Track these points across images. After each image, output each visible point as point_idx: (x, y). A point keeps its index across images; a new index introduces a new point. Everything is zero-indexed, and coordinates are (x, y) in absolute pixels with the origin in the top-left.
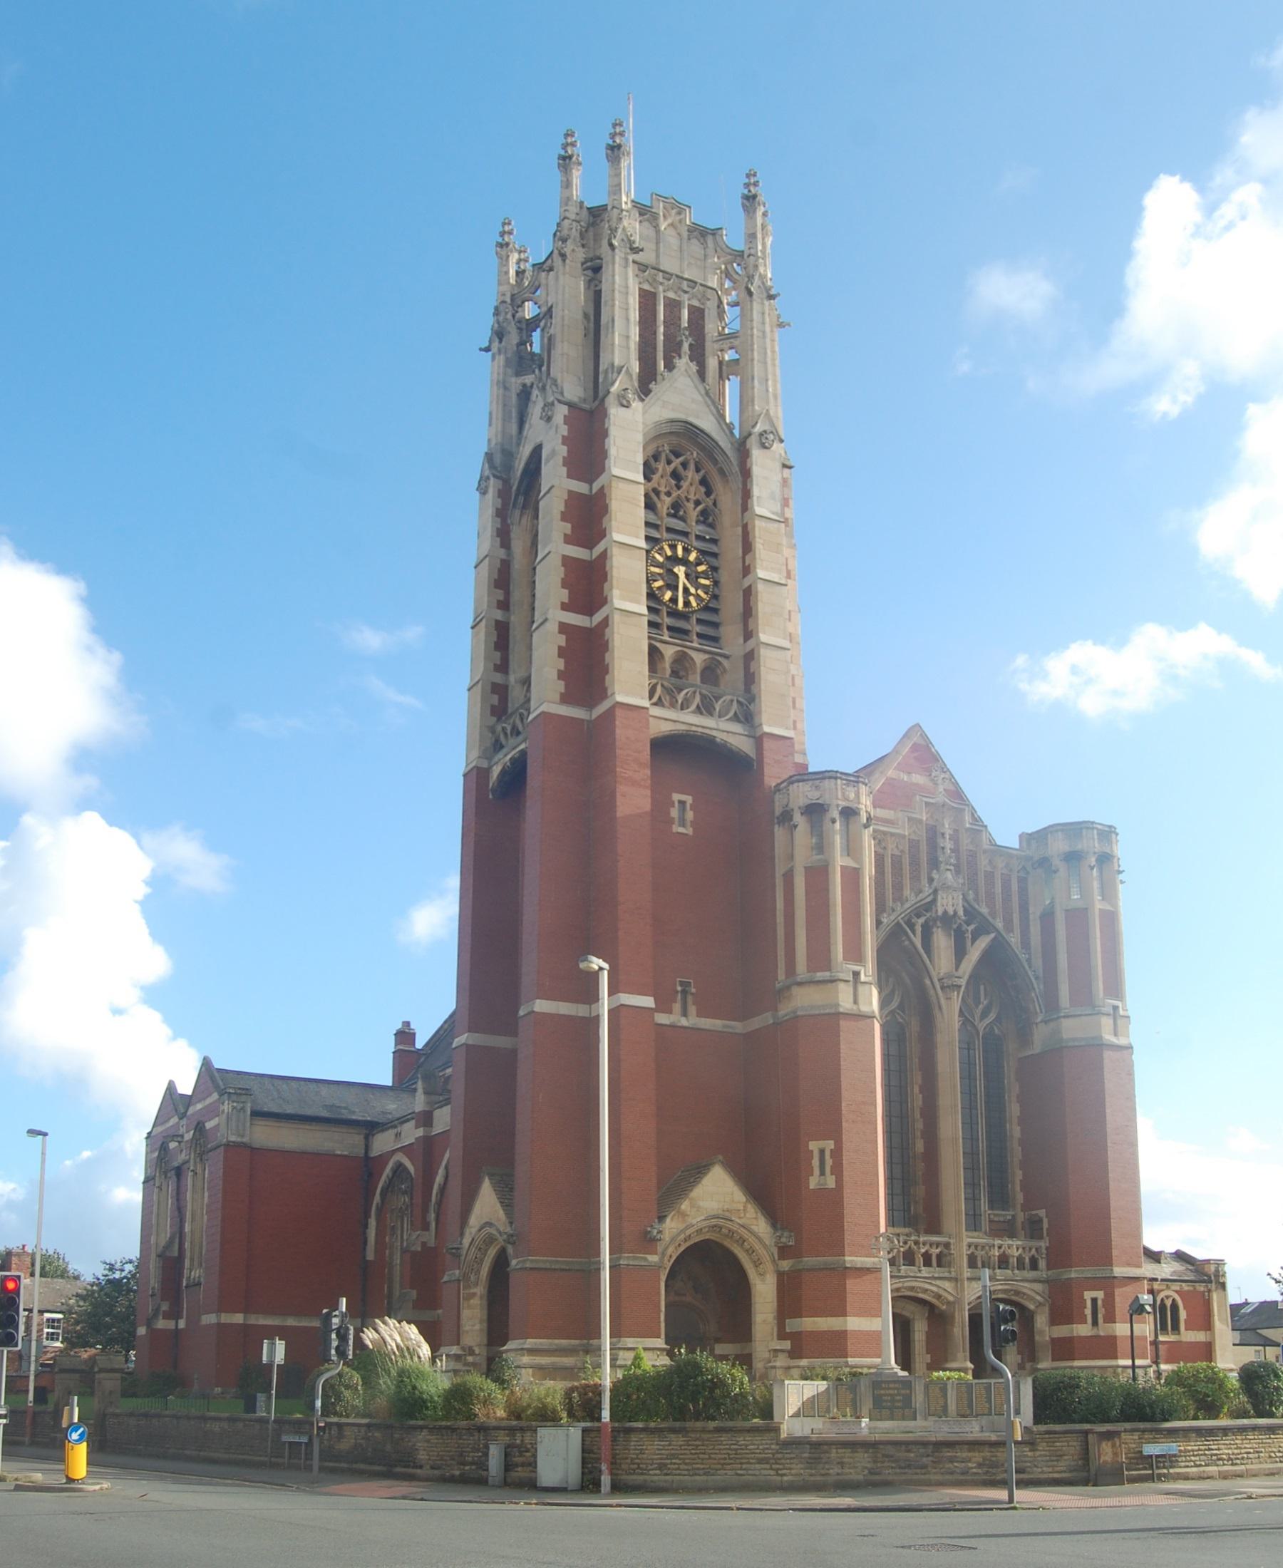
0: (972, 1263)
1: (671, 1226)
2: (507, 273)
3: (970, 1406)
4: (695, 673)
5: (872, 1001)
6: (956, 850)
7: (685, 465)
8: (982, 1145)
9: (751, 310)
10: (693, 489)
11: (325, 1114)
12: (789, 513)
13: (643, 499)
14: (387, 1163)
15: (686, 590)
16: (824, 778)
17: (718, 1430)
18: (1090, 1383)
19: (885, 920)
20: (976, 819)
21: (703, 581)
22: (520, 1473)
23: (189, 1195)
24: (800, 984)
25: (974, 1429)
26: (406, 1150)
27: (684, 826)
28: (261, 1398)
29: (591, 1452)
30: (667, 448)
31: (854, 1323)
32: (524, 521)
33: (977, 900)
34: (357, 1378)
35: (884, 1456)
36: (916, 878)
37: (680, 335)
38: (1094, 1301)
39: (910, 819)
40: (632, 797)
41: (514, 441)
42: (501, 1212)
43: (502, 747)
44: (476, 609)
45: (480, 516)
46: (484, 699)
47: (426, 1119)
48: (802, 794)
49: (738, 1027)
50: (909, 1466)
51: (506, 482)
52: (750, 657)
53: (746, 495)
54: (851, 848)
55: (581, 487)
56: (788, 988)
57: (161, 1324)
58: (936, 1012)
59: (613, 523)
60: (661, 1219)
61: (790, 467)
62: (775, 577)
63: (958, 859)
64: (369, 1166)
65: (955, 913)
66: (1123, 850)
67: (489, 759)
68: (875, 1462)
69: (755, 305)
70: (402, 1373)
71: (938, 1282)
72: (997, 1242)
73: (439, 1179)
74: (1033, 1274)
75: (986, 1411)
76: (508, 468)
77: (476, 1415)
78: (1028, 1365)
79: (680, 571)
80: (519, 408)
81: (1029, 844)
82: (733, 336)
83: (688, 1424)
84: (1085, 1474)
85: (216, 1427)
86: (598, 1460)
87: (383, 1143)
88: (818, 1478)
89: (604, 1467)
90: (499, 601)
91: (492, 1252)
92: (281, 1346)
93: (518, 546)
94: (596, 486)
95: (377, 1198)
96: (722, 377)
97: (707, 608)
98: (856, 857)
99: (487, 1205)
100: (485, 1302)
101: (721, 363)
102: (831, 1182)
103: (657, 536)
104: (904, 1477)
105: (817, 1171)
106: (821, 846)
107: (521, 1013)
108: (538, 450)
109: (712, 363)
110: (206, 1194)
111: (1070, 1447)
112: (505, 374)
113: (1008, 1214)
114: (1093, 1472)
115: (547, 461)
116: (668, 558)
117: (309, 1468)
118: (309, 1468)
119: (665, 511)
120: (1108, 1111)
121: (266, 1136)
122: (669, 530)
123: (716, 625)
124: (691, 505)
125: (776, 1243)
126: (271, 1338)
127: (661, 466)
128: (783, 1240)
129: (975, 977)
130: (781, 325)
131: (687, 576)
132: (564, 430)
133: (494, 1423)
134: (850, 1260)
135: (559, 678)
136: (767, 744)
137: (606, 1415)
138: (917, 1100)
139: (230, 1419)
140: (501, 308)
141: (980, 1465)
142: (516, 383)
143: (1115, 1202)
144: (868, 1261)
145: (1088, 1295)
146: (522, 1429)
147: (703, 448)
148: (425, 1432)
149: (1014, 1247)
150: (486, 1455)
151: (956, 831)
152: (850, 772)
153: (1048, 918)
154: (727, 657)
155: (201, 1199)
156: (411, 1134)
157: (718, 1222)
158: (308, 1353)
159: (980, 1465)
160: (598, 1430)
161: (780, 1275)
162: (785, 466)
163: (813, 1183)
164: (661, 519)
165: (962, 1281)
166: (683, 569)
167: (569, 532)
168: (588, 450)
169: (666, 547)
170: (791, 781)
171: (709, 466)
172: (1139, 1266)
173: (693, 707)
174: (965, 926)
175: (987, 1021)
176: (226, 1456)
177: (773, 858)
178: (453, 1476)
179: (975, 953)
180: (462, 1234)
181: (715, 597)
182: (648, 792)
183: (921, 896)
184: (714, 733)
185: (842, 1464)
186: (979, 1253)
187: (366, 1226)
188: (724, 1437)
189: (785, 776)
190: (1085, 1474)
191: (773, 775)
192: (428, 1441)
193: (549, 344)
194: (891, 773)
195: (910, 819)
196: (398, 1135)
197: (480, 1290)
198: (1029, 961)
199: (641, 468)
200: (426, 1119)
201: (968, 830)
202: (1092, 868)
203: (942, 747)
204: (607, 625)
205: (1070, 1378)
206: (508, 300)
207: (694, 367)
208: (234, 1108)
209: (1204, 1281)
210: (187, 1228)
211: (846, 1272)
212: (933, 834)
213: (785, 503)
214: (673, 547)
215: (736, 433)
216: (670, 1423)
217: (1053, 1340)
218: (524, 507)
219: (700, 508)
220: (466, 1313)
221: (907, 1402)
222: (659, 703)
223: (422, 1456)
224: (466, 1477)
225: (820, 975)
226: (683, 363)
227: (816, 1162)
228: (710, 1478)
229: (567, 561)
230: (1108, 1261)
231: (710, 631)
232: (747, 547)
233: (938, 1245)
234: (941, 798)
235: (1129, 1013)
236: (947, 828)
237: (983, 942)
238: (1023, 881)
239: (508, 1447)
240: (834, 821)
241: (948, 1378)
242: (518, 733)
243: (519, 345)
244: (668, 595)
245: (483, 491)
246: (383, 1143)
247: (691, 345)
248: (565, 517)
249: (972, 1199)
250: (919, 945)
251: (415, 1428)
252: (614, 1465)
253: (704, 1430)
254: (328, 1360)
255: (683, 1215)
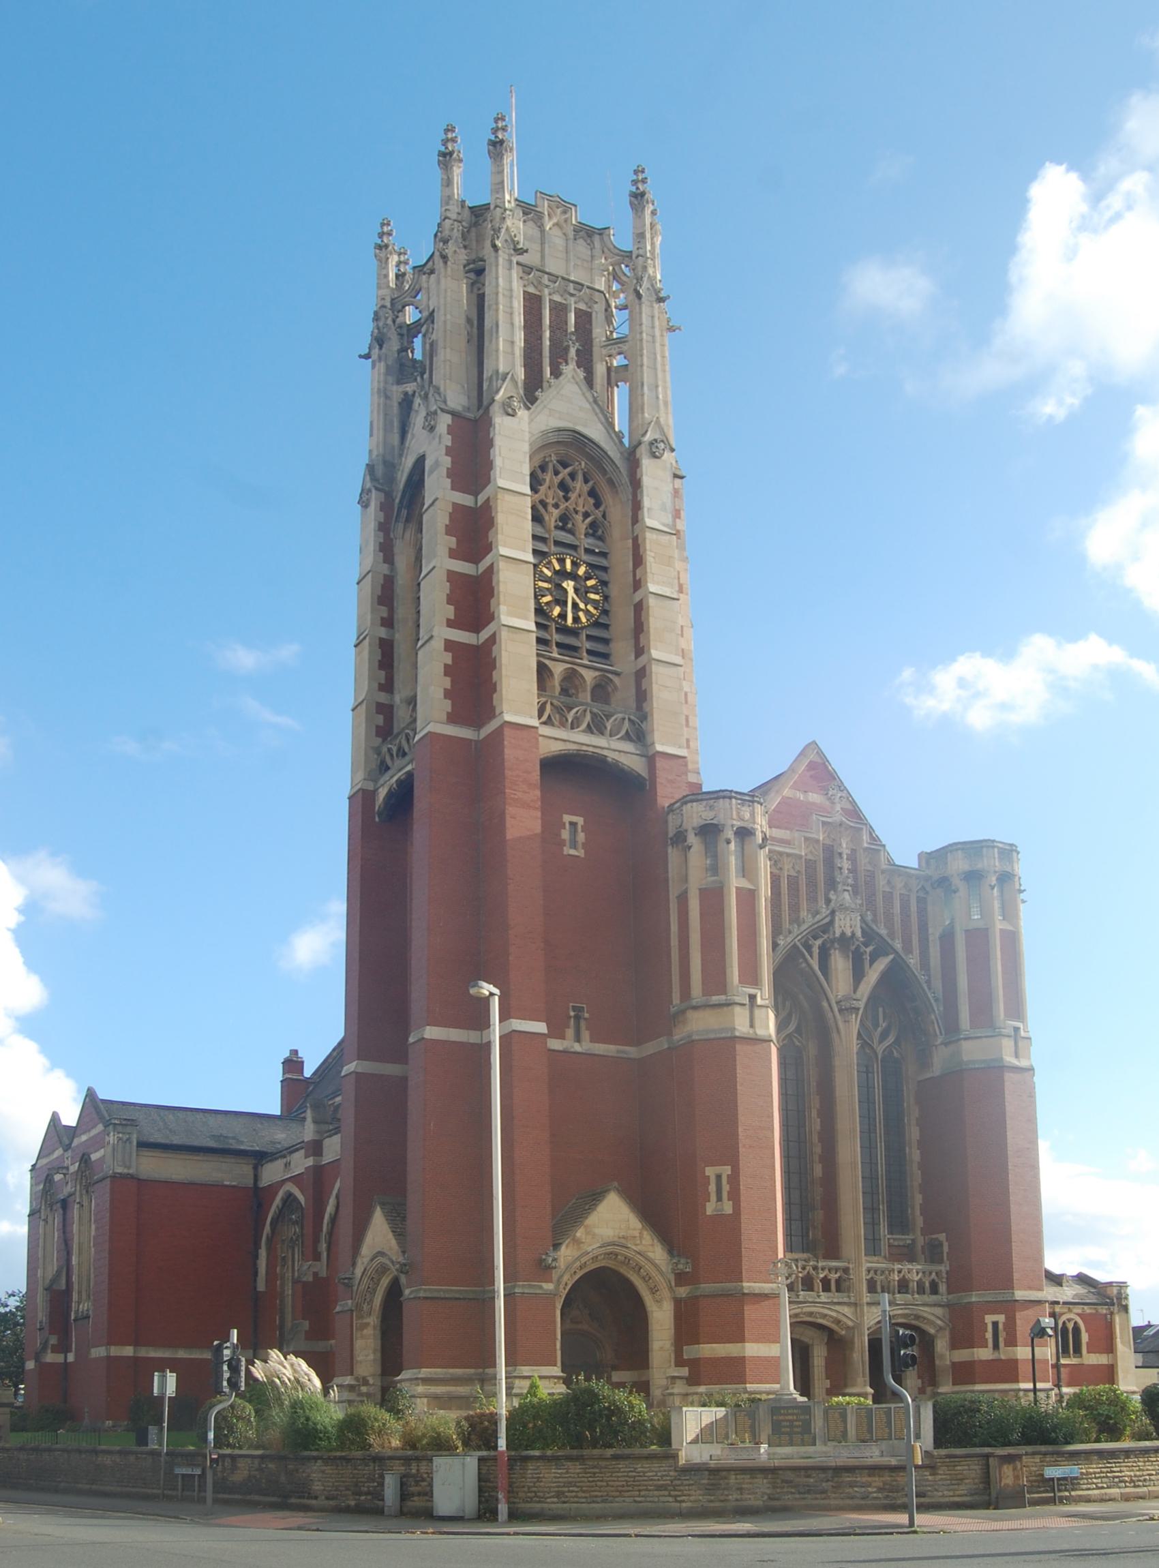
0: (872, 1287)
1: (566, 1254)
2: (386, 276)
3: (870, 1431)
4: (585, 691)
5: (769, 1024)
6: (854, 870)
7: (573, 476)
8: (881, 1168)
9: (641, 313)
10: (581, 501)
11: (212, 1144)
12: (680, 525)
13: (530, 511)
14: (276, 1193)
15: (575, 605)
16: (718, 798)
17: (616, 1457)
18: (990, 1404)
19: (781, 943)
20: (874, 839)
21: (592, 596)
22: (417, 1503)
23: (75, 1227)
24: (695, 1008)
25: (873, 1454)
26: (296, 1180)
27: (575, 848)
28: (153, 1430)
29: (488, 1481)
30: (554, 458)
31: (752, 1349)
32: (407, 535)
33: (875, 921)
34: (249, 1409)
35: (783, 1481)
36: (812, 899)
37: (566, 341)
38: (995, 1324)
39: (806, 839)
40: (522, 818)
41: (396, 451)
42: (394, 1242)
43: (388, 768)
44: (359, 627)
45: (363, 529)
46: (369, 720)
47: (316, 1148)
48: (696, 814)
49: (632, 1052)
50: (809, 1492)
51: (389, 495)
52: (641, 674)
53: (637, 506)
54: (746, 870)
55: (466, 500)
56: (683, 1012)
57: (50, 1358)
58: (835, 1035)
59: (500, 536)
60: (556, 1246)
61: (682, 478)
62: (667, 592)
63: (855, 879)
64: (258, 1196)
65: (853, 934)
66: (1024, 868)
67: (375, 781)
68: (774, 1487)
69: (645, 309)
70: (296, 1405)
71: (837, 1308)
72: (897, 1266)
73: (330, 1209)
74: (934, 1298)
75: (886, 1436)
76: (390, 479)
77: (370, 1446)
78: (929, 1389)
79: (569, 585)
80: (400, 417)
81: (928, 863)
82: (622, 340)
83: (586, 1452)
84: (987, 1498)
85: (107, 1460)
86: (495, 1489)
87: (272, 1173)
88: (717, 1504)
89: (500, 1496)
90: (382, 619)
91: (385, 1282)
92: (171, 1379)
93: (402, 561)
94: (481, 498)
95: (267, 1229)
96: (610, 383)
97: (597, 624)
98: (751, 878)
99: (380, 1233)
100: (378, 1332)
101: (609, 369)
102: (728, 1208)
103: (546, 550)
104: (803, 1503)
105: (713, 1197)
106: (716, 867)
107: (411, 1040)
108: (421, 460)
109: (600, 369)
110: (93, 1227)
111: (971, 1471)
112: (386, 382)
113: (908, 1239)
114: (994, 1494)
115: (431, 472)
116: (556, 572)
117: (202, 1500)
118: (202, 1500)
119: (553, 524)
120: (1009, 1134)
121: (153, 1167)
122: (557, 543)
123: (606, 641)
124: (579, 518)
125: (673, 1270)
126: (162, 1370)
127: (548, 477)
128: (680, 1266)
129: (873, 999)
130: (671, 329)
131: (576, 590)
132: (448, 441)
133: (390, 1453)
134: (748, 1286)
135: (445, 697)
136: (660, 763)
137: (502, 1443)
138: (816, 1124)
139: (120, 1452)
140: (381, 314)
141: (880, 1490)
142: (397, 392)
143: (1017, 1225)
144: (766, 1287)
145: (989, 1319)
146: (417, 1459)
147: (590, 458)
148: (319, 1462)
149: (914, 1271)
150: (382, 1484)
151: (854, 851)
152: (746, 791)
153: (948, 939)
154: (617, 674)
155: (88, 1230)
156: (301, 1163)
157: (614, 1249)
158: (200, 1384)
159: (880, 1490)
160: (495, 1459)
161: (678, 1302)
162: (676, 476)
163: (710, 1208)
164: (549, 531)
165: (862, 1305)
166: (571, 583)
167: (454, 546)
168: (473, 465)
169: (554, 561)
170: (684, 801)
171: (598, 477)
172: (1041, 1289)
173: (584, 726)
174: (863, 948)
175: (886, 1044)
176: (119, 1489)
177: (666, 880)
178: (349, 1506)
179: (873, 975)
180: (354, 1264)
181: (605, 612)
182: (539, 814)
183: (818, 917)
184: (605, 753)
185: (740, 1489)
186: (879, 1278)
187: (256, 1257)
188: (621, 1465)
189: (678, 796)
190: (987, 1498)
191: (666, 795)
192: (323, 1472)
193: (431, 351)
194: (787, 792)
195: (806, 839)
196: (287, 1165)
197: (373, 1320)
198: (928, 982)
199: (528, 478)
200: (316, 1148)
202: (993, 888)
203: (837, 763)
204: (494, 643)
205: (972, 1402)
206: (388, 305)
207: (581, 374)
208: (120, 1139)
209: (1106, 1304)
210: (74, 1261)
211: (744, 1297)
212: (830, 854)
213: (677, 514)
214: (562, 561)
215: (626, 441)
216: (568, 1451)
217: (954, 1364)
218: (407, 521)
219: (589, 520)
220: (359, 1344)
221: (807, 1428)
222: (548, 722)
223: (317, 1487)
224: (361, 1507)
225: (715, 999)
226: (570, 369)
227: (712, 1188)
228: (607, 1505)
229: (452, 576)
230: (1009, 1284)
231: (600, 648)
232: (638, 560)
233: (837, 1270)
234: (838, 817)
235: (1031, 1034)
236: (845, 846)
237: (882, 964)
238: (922, 901)
239: (403, 1476)
240: (728, 842)
241: (848, 1403)
242: (404, 754)
243: (399, 351)
244: (557, 611)
245: (364, 504)
246: (272, 1173)
247: (578, 350)
248: (449, 531)
249: (872, 1224)
250: (816, 967)
251: (309, 1459)
252: (511, 1492)
253: (601, 1458)
254: (220, 1392)
255: (578, 1242)
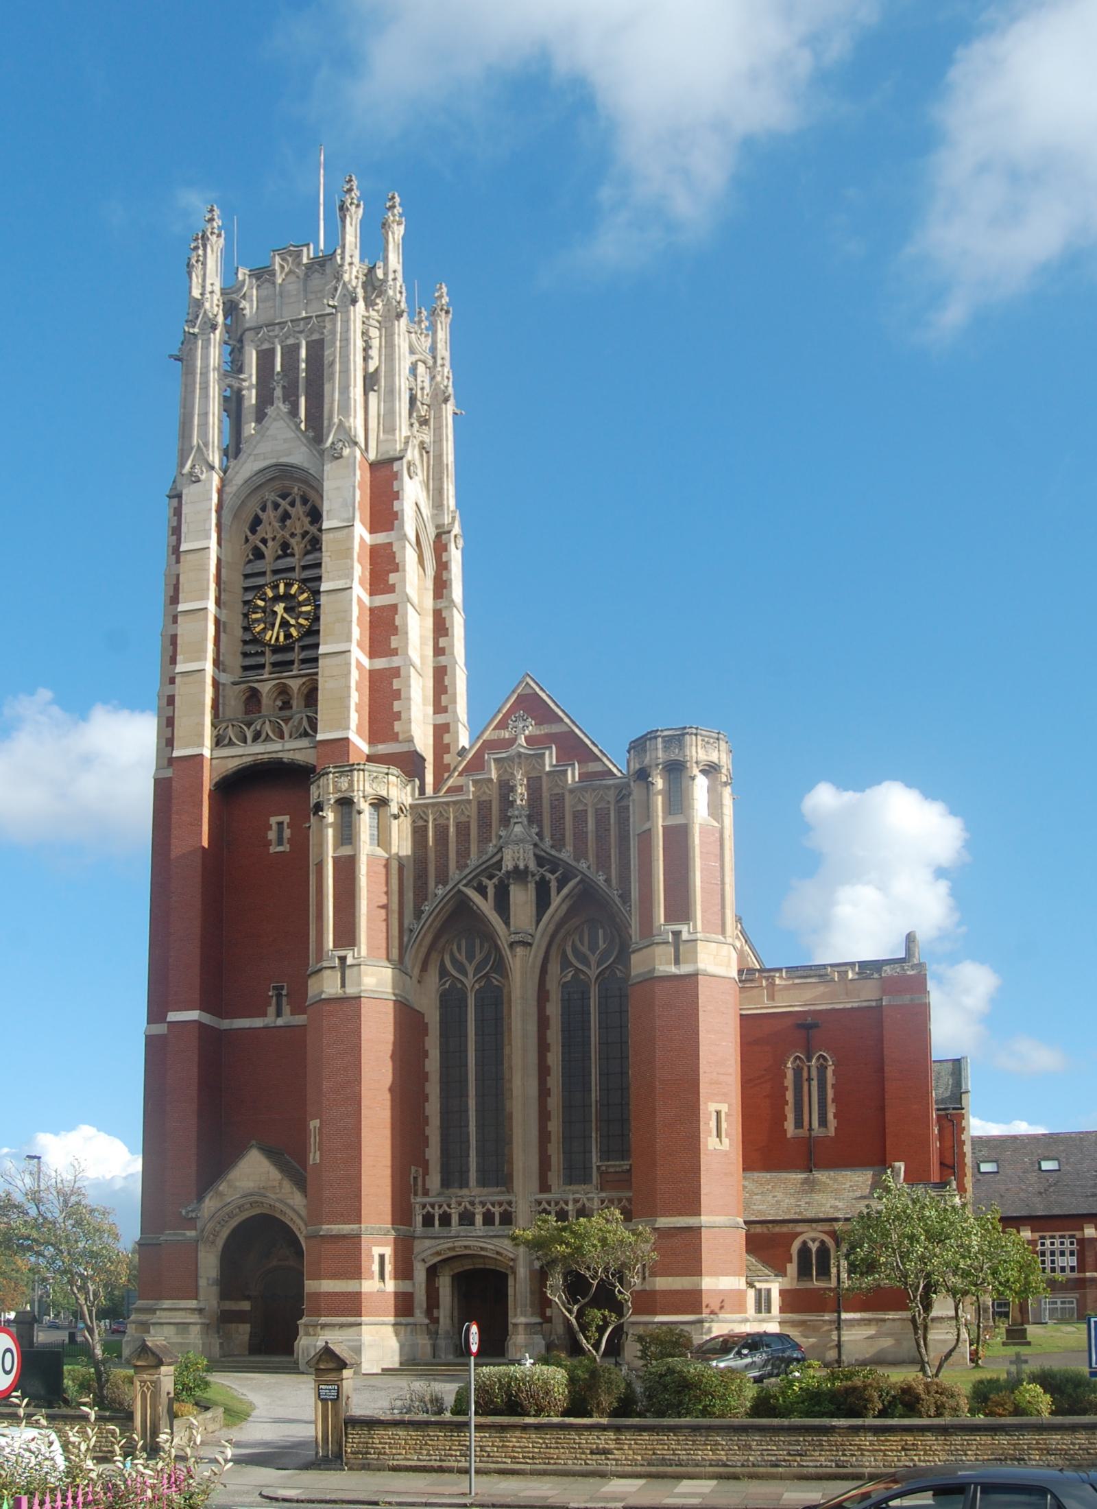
65: (526, 867)
184: (280, 755)
201: (550, 772)
219: (308, 537)
